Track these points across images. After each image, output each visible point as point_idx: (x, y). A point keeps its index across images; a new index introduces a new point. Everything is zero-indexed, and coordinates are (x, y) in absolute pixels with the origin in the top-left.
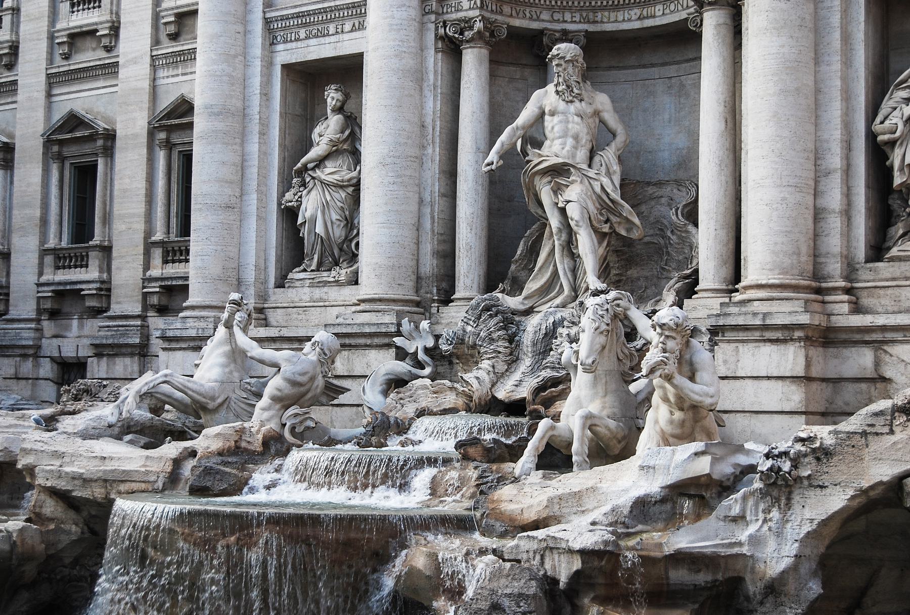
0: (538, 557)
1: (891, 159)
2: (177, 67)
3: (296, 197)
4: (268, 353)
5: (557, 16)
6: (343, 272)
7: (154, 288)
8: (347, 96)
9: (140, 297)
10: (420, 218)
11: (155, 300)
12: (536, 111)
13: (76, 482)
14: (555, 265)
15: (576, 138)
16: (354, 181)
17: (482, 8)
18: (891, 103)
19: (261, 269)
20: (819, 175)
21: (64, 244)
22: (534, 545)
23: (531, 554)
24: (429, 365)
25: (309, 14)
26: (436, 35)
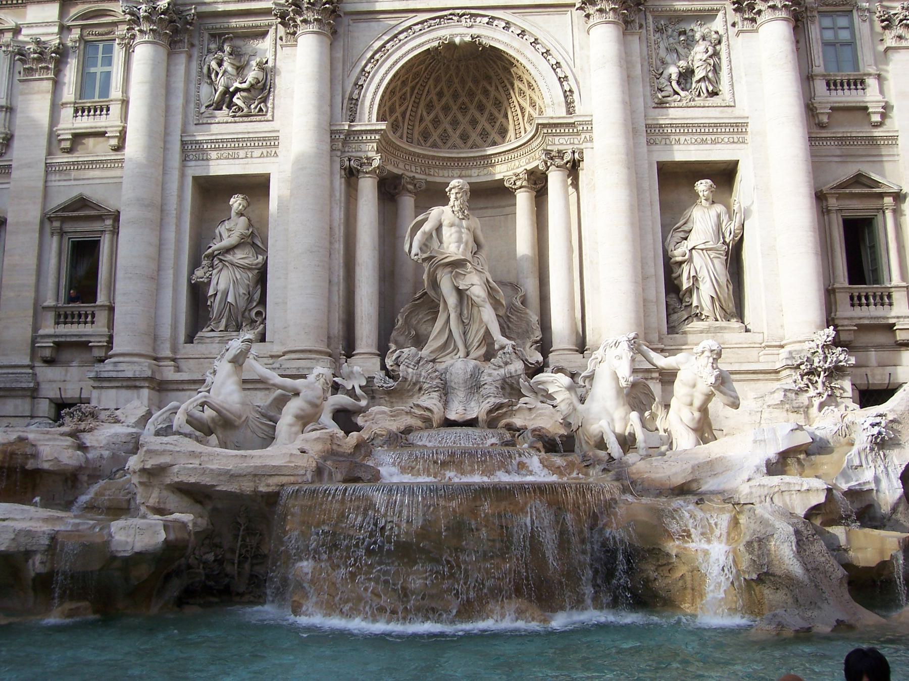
0: (768, 499)
1: (679, 272)
3: (207, 275)
4: (288, 381)
8: (249, 205)
9: (29, 351)
10: (330, 291)
11: (47, 353)
12: (438, 225)
13: (221, 478)
14: (450, 331)
15: (466, 244)
16: (260, 266)
18: (676, 240)
19: (174, 327)
20: (645, 278)
23: (763, 498)
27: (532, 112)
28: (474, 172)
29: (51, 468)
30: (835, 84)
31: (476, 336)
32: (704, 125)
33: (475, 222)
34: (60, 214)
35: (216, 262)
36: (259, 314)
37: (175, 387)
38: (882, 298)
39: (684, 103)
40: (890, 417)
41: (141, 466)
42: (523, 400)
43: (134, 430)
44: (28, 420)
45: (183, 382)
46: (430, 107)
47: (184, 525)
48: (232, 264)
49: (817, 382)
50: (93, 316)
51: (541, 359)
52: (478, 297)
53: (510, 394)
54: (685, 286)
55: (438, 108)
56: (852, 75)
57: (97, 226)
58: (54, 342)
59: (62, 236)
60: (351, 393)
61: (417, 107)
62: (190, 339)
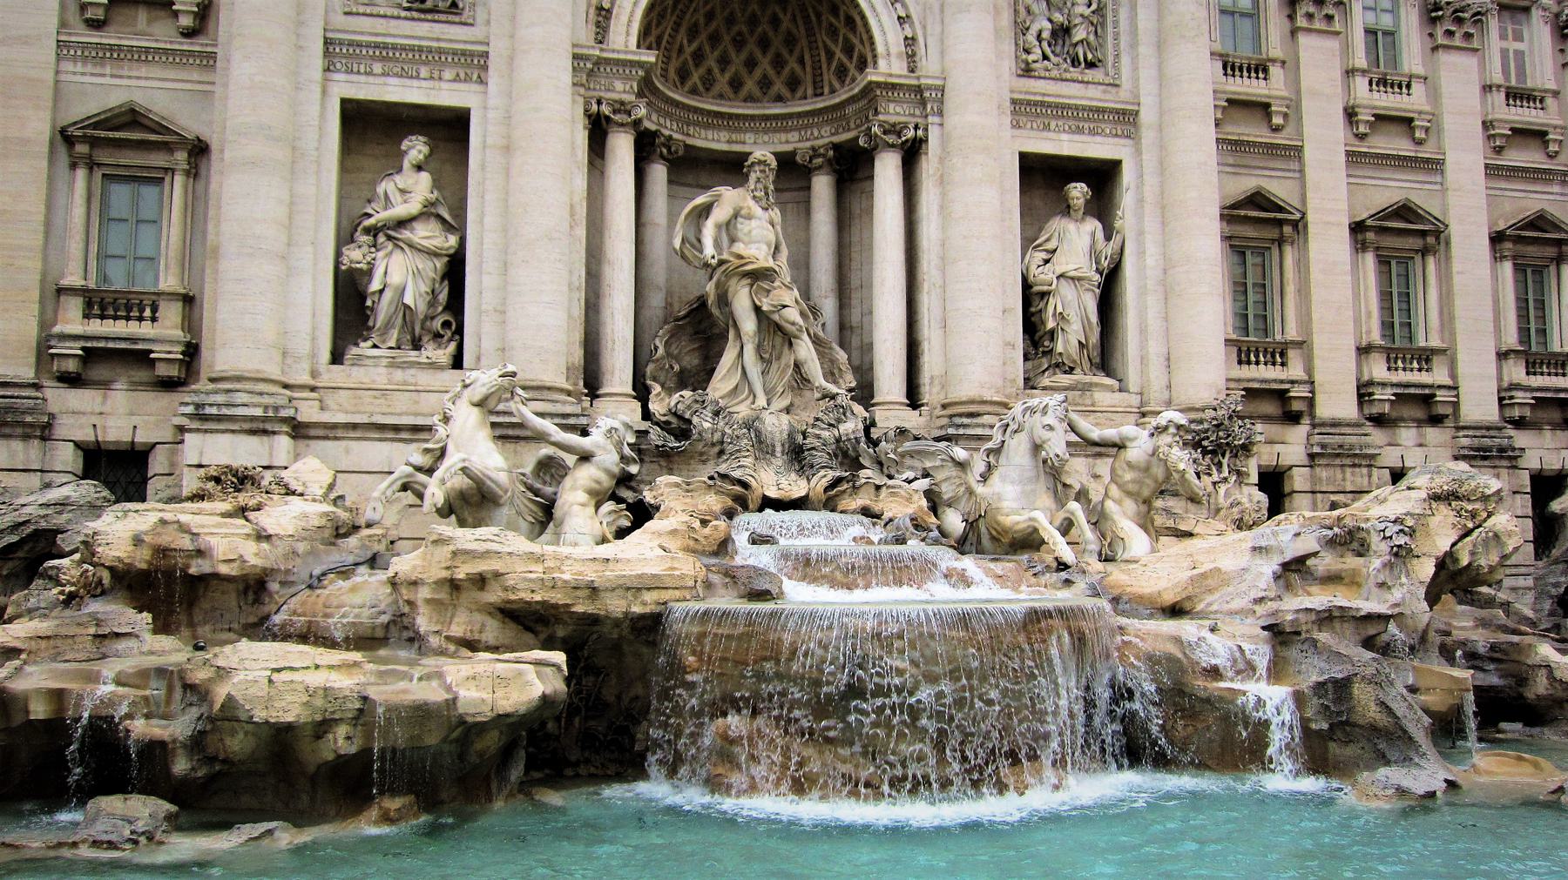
1: (1042, 305)
2: (103, 65)
4: (573, 439)
5: (662, 121)
6: (440, 352)
7: (75, 349)
9: (33, 360)
10: (570, 300)
11: (71, 366)
12: (731, 212)
14: (743, 368)
15: (769, 246)
16: (452, 251)
17: (640, 95)
22: (1313, 617)
24: (635, 461)
25: (394, 47)
26: (586, 110)
27: (845, 60)
28: (749, 138)
29: (234, 573)
30: (1233, 69)
31: (782, 376)
32: (1084, 108)
34: (90, 132)
35: (381, 239)
36: (446, 324)
37: (321, 432)
38: (1273, 356)
39: (1055, 73)
40: (1410, 522)
41: (445, 574)
42: (863, 473)
44: (35, 480)
45: (334, 426)
46: (693, 33)
47: (559, 668)
48: (411, 246)
49: (1219, 465)
50: (155, 309)
52: (793, 324)
53: (841, 464)
54: (1050, 325)
55: (703, 37)
56: (1255, 58)
57: (158, 160)
58: (83, 349)
59: (91, 169)
61: (676, 30)
62: (337, 358)
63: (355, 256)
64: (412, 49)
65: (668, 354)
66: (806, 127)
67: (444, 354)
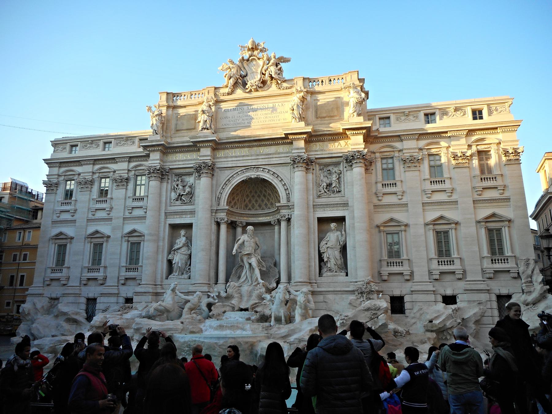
4: (187, 297)
11: (123, 282)
21: (90, 265)
28: (263, 218)
30: (385, 185)
32: (333, 204)
33: (257, 239)
38: (399, 263)
39: (327, 196)
42: (264, 301)
43: (140, 312)
46: (248, 196)
51: (275, 285)
54: (325, 260)
55: (250, 196)
60: (213, 297)
63: (170, 257)
64: (181, 212)
65: (236, 272)
66: (273, 215)
67: (186, 276)
